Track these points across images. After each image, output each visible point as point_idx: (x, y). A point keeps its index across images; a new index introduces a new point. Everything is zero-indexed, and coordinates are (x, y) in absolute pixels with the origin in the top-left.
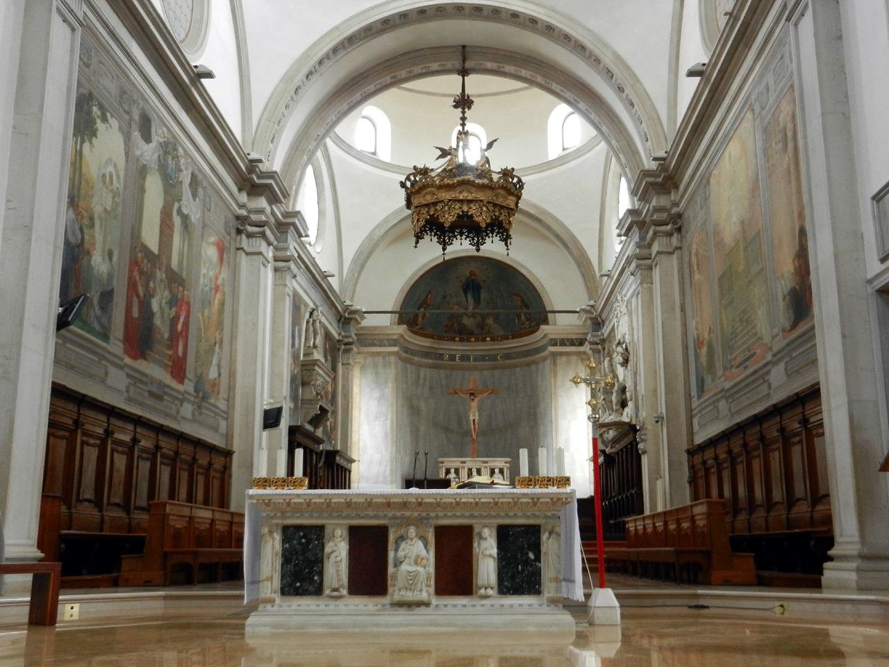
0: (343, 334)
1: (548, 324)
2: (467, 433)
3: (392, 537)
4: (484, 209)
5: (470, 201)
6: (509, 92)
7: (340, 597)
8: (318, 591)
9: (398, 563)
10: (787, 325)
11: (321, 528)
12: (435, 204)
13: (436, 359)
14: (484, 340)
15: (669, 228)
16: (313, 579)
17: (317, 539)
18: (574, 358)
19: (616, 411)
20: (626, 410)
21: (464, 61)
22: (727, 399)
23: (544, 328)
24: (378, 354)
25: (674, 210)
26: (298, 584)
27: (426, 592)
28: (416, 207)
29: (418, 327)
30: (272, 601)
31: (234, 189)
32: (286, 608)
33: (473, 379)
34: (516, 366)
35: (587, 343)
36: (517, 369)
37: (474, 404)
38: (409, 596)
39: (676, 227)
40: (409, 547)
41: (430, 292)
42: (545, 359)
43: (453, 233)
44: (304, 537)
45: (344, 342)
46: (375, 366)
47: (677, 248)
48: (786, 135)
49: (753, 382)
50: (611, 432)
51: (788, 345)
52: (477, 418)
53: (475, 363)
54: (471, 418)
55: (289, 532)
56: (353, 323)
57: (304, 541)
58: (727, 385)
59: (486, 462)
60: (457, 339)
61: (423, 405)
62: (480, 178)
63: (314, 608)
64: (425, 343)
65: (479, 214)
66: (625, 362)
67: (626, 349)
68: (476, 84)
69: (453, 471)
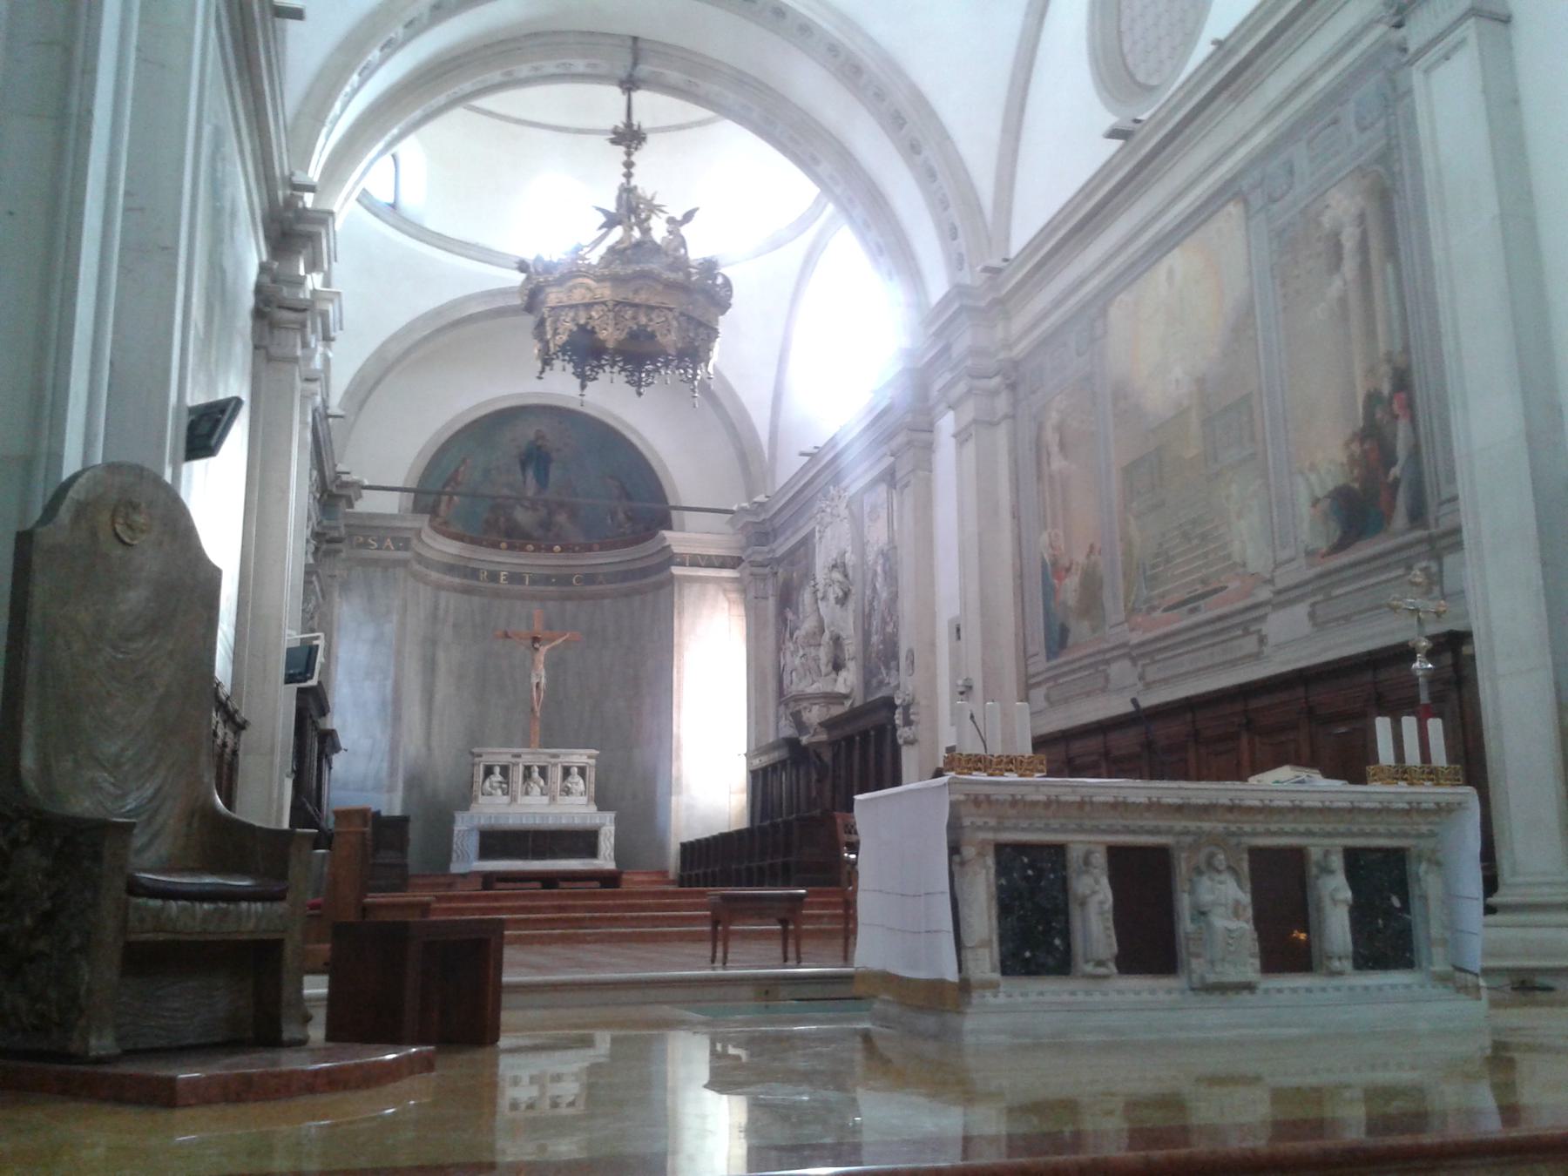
0: (325, 522)
1: (670, 528)
3: (1182, 868)
4: (675, 323)
5: (652, 308)
6: (680, 127)
7: (1105, 977)
8: (1063, 966)
9: (1201, 913)
10: (1322, 545)
11: (1060, 850)
12: (588, 306)
13: (465, 576)
14: (550, 549)
15: (995, 382)
16: (1051, 944)
17: (1053, 870)
18: (711, 589)
19: (826, 675)
20: (843, 674)
21: (635, 64)
22: (1134, 660)
24: (375, 562)
26: (1028, 954)
27: (1250, 969)
28: (553, 308)
29: (439, 520)
30: (992, 986)
32: (1021, 999)
34: (603, 596)
35: (743, 565)
36: (606, 602)
38: (1232, 975)
39: (1008, 382)
40: (1219, 886)
41: (464, 461)
43: (599, 361)
44: (1031, 866)
45: (327, 537)
47: (1006, 417)
48: (1338, 246)
49: (1192, 640)
50: (816, 709)
51: (1321, 576)
52: (543, 681)
53: (531, 588)
54: (534, 681)
55: (1008, 855)
56: (343, 503)
57: (1030, 872)
58: (1135, 638)
59: (555, 756)
60: (503, 545)
62: (673, 271)
63: (1066, 998)
65: (665, 332)
67: (846, 576)
68: (650, 106)
69: (497, 770)
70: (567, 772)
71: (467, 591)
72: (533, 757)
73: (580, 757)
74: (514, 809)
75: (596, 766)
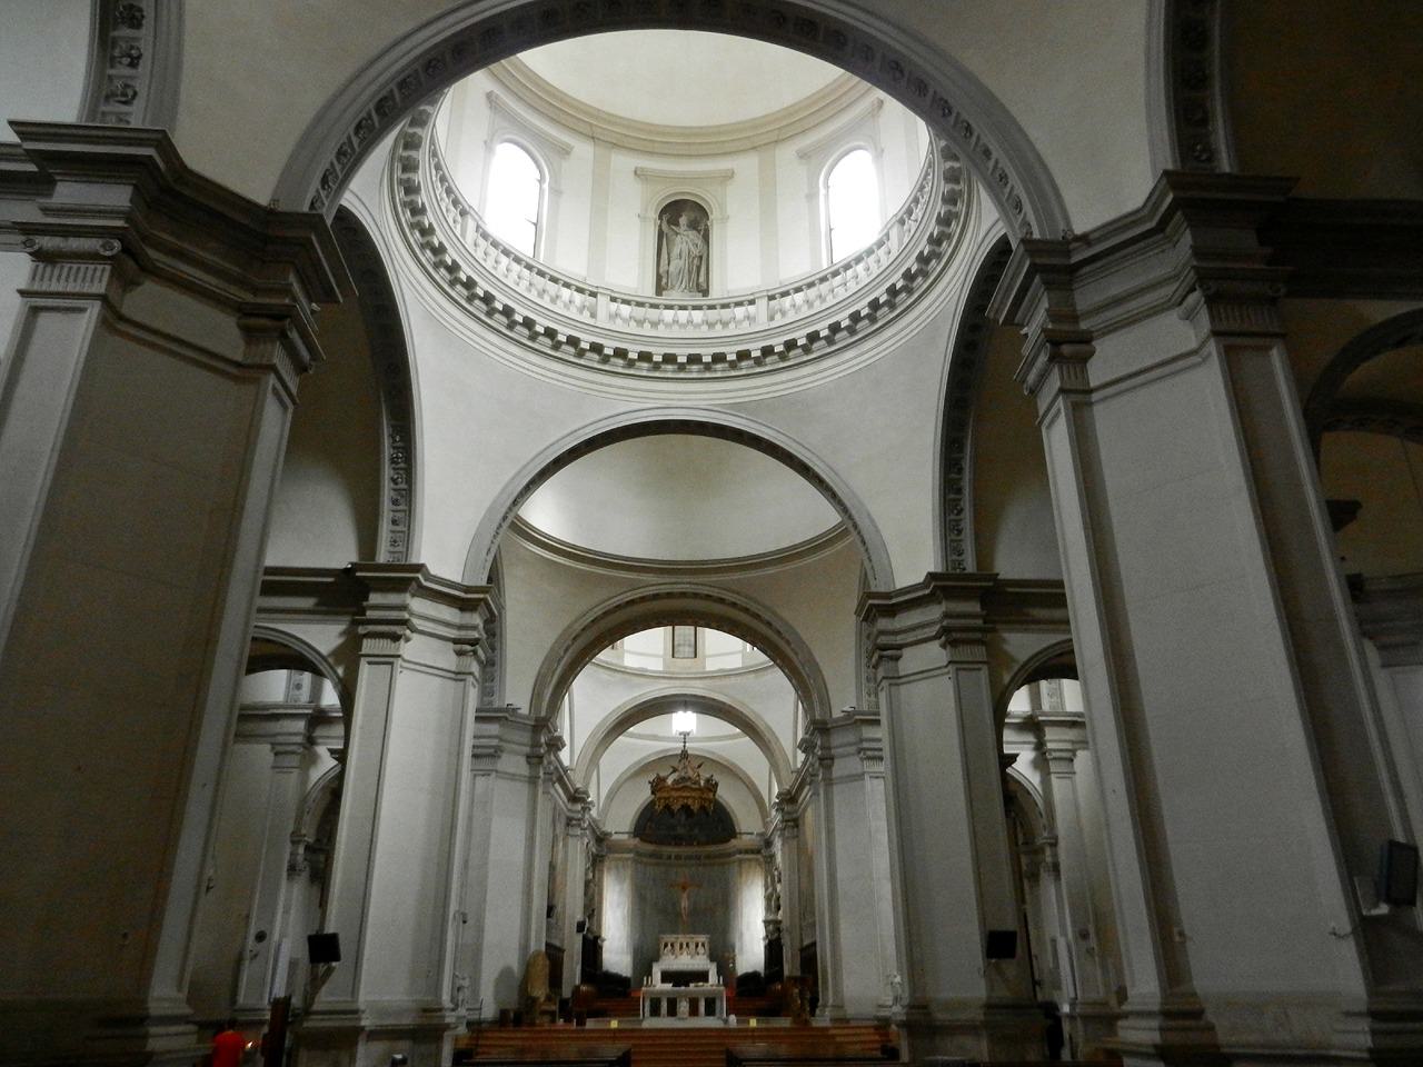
1: (735, 837)
2: (678, 915)
12: (669, 798)
14: (692, 844)
18: (753, 864)
23: (734, 842)
24: (620, 859)
25: (795, 815)
27: (687, 1015)
31: (566, 801)
37: (685, 895)
46: (617, 868)
54: (683, 905)
61: (648, 896)
64: (650, 848)
66: (780, 881)
70: (697, 946)
71: (657, 864)
72: (682, 939)
73: (702, 938)
74: (677, 961)
75: (709, 943)
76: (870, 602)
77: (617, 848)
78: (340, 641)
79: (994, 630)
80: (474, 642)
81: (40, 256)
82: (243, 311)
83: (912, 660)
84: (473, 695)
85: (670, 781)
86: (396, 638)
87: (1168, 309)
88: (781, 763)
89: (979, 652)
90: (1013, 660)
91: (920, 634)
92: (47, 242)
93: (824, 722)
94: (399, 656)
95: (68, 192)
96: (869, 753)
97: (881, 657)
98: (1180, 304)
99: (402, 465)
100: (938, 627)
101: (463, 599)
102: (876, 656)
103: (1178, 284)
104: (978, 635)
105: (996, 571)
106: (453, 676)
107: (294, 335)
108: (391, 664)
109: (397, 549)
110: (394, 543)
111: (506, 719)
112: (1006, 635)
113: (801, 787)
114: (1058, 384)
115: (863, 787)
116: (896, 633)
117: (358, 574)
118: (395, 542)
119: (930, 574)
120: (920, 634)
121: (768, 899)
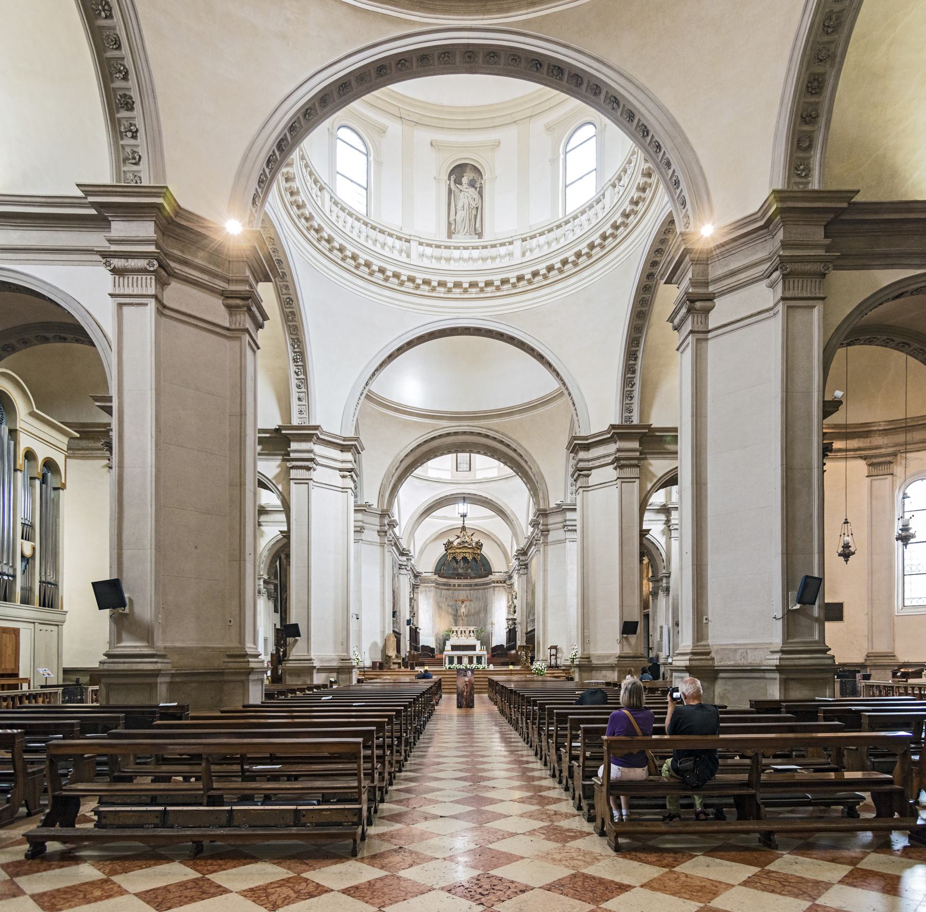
23: (490, 576)
24: (427, 587)
33: (462, 594)
37: (463, 606)
42: (490, 588)
46: (426, 591)
76: (576, 442)
77: (425, 581)
78: (278, 470)
79: (645, 459)
80: (350, 470)
81: (115, 271)
82: (225, 295)
83: (596, 477)
84: (352, 499)
85: (455, 544)
86: (308, 469)
87: (761, 280)
88: (519, 532)
89: (635, 472)
90: (654, 476)
91: (603, 461)
92: (118, 263)
93: (545, 510)
94: (311, 479)
95: (120, 228)
96: (570, 528)
97: (579, 475)
98: (769, 277)
99: (300, 363)
100: (613, 457)
101: (342, 445)
102: (576, 475)
103: (769, 264)
104: (635, 462)
105: (651, 423)
106: (341, 490)
107: (254, 309)
108: (308, 483)
109: (303, 416)
110: (301, 412)
111: (365, 510)
112: (652, 462)
113: (530, 546)
114: (690, 328)
115: (565, 547)
116: (588, 461)
117: (283, 432)
118: (301, 411)
119: (611, 425)
120: (603, 461)
121: (509, 607)
